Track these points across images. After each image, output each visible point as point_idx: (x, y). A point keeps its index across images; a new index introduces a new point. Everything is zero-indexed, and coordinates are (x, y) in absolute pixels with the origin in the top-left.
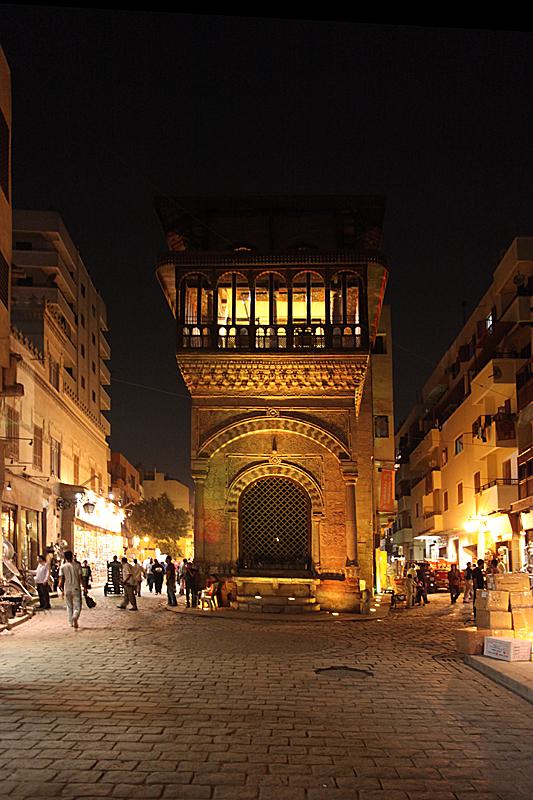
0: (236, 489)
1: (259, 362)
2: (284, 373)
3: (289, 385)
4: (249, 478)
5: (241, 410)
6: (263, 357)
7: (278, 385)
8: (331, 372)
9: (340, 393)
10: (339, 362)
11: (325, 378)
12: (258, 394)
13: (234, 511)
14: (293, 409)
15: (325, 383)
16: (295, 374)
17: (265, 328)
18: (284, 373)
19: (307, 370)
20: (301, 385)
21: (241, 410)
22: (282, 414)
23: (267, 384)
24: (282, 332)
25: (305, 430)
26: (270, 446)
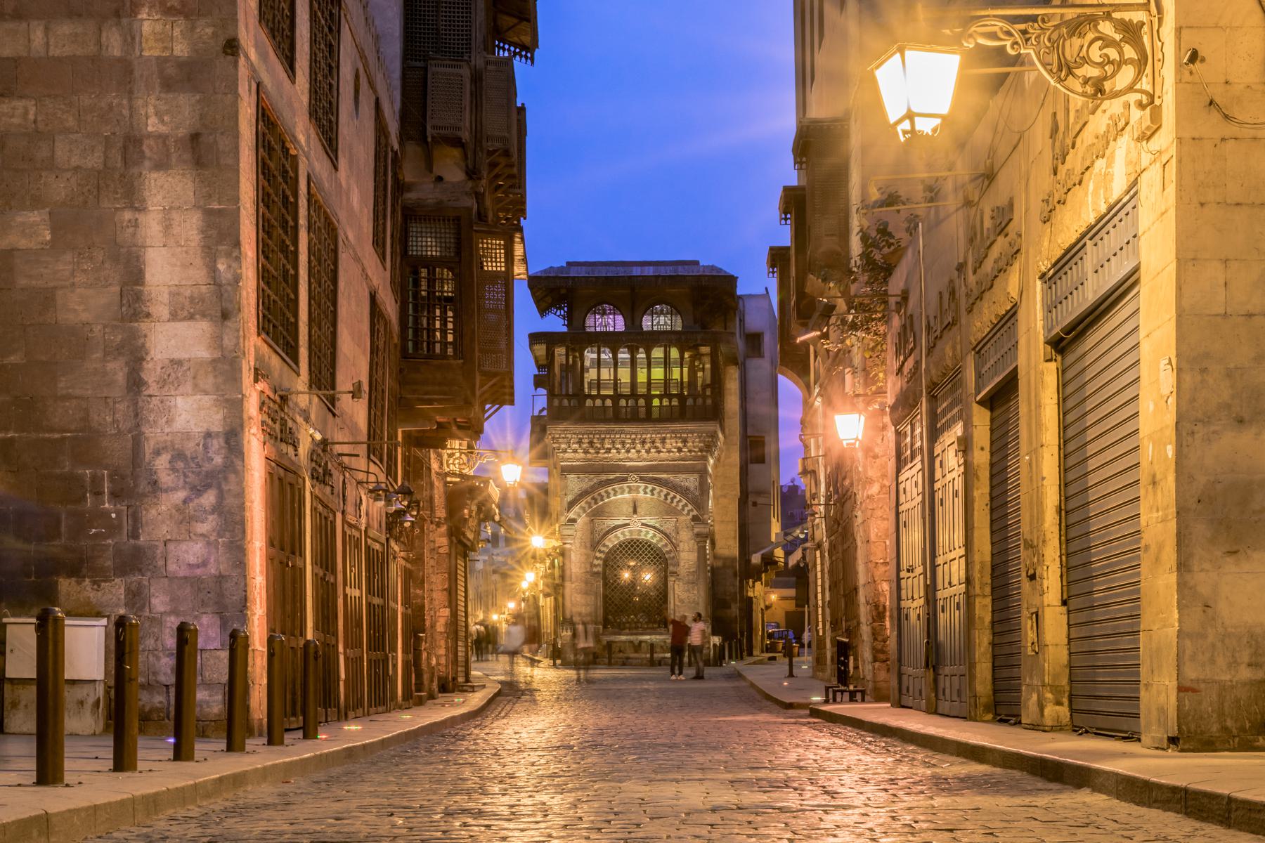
0: (600, 552)
1: (621, 432)
2: (643, 442)
3: (648, 452)
4: (611, 541)
5: (604, 477)
6: (626, 428)
7: (639, 452)
8: (685, 441)
9: (694, 458)
10: (692, 432)
11: (680, 445)
12: (621, 460)
13: (597, 573)
14: (650, 475)
15: (680, 450)
16: (653, 442)
17: (626, 397)
18: (643, 442)
19: (665, 438)
20: (659, 452)
21: (604, 477)
22: (642, 479)
23: (628, 451)
24: (642, 402)
25: (662, 495)
26: (631, 510)
